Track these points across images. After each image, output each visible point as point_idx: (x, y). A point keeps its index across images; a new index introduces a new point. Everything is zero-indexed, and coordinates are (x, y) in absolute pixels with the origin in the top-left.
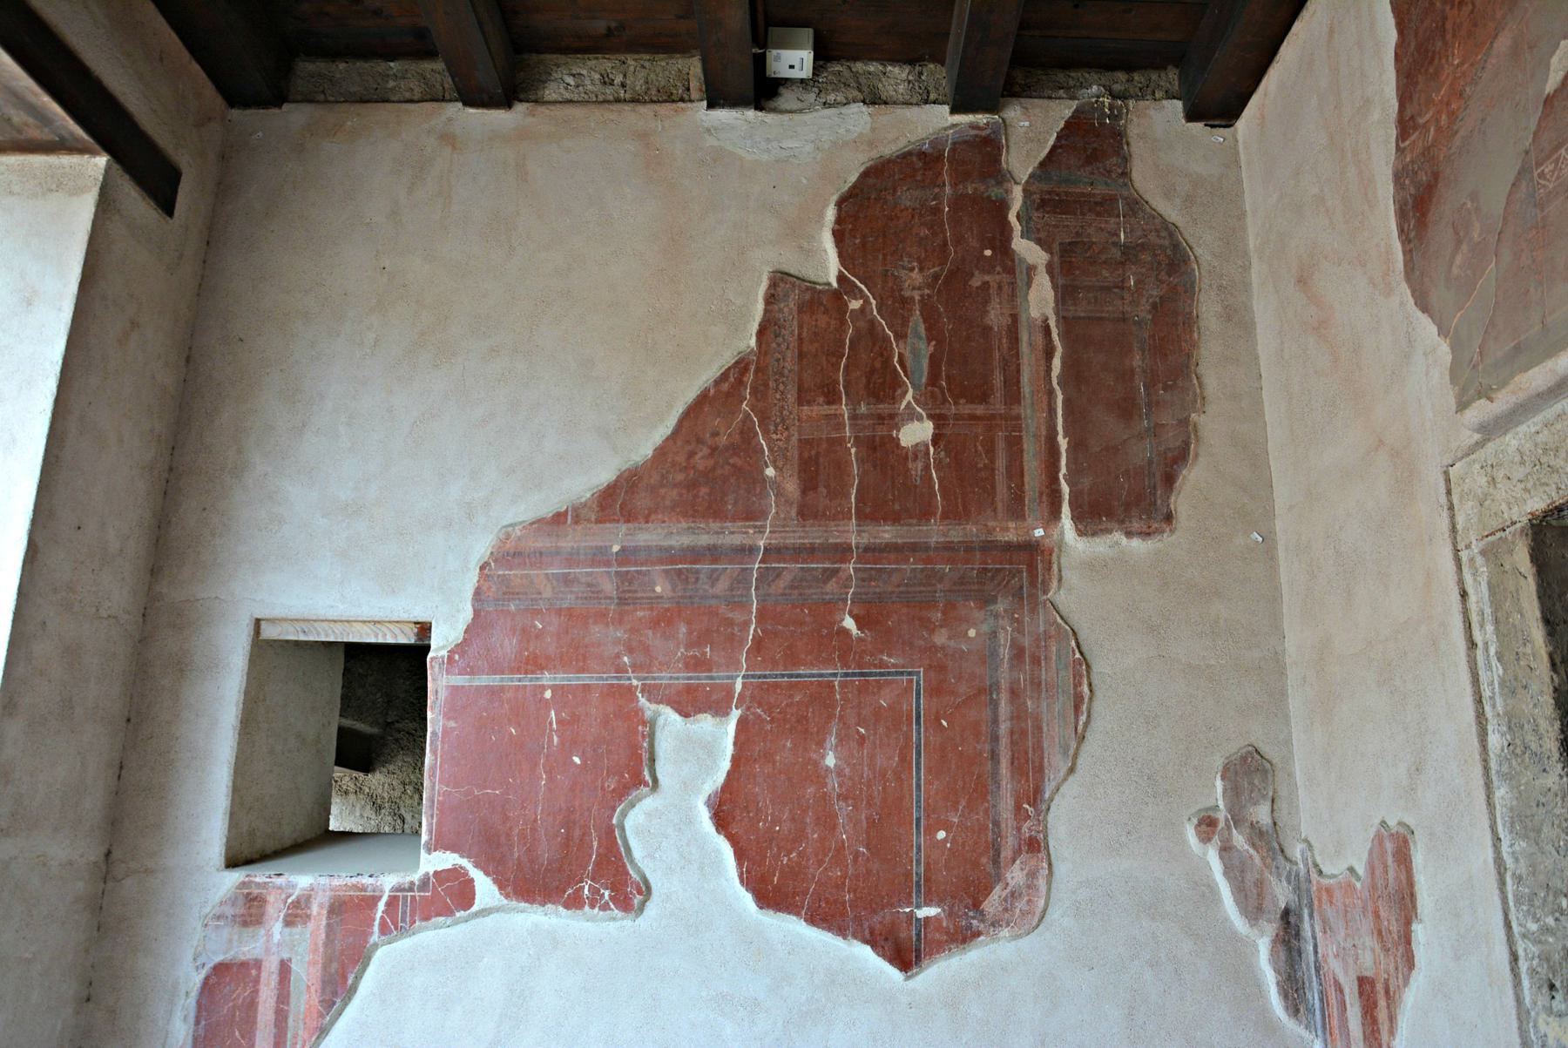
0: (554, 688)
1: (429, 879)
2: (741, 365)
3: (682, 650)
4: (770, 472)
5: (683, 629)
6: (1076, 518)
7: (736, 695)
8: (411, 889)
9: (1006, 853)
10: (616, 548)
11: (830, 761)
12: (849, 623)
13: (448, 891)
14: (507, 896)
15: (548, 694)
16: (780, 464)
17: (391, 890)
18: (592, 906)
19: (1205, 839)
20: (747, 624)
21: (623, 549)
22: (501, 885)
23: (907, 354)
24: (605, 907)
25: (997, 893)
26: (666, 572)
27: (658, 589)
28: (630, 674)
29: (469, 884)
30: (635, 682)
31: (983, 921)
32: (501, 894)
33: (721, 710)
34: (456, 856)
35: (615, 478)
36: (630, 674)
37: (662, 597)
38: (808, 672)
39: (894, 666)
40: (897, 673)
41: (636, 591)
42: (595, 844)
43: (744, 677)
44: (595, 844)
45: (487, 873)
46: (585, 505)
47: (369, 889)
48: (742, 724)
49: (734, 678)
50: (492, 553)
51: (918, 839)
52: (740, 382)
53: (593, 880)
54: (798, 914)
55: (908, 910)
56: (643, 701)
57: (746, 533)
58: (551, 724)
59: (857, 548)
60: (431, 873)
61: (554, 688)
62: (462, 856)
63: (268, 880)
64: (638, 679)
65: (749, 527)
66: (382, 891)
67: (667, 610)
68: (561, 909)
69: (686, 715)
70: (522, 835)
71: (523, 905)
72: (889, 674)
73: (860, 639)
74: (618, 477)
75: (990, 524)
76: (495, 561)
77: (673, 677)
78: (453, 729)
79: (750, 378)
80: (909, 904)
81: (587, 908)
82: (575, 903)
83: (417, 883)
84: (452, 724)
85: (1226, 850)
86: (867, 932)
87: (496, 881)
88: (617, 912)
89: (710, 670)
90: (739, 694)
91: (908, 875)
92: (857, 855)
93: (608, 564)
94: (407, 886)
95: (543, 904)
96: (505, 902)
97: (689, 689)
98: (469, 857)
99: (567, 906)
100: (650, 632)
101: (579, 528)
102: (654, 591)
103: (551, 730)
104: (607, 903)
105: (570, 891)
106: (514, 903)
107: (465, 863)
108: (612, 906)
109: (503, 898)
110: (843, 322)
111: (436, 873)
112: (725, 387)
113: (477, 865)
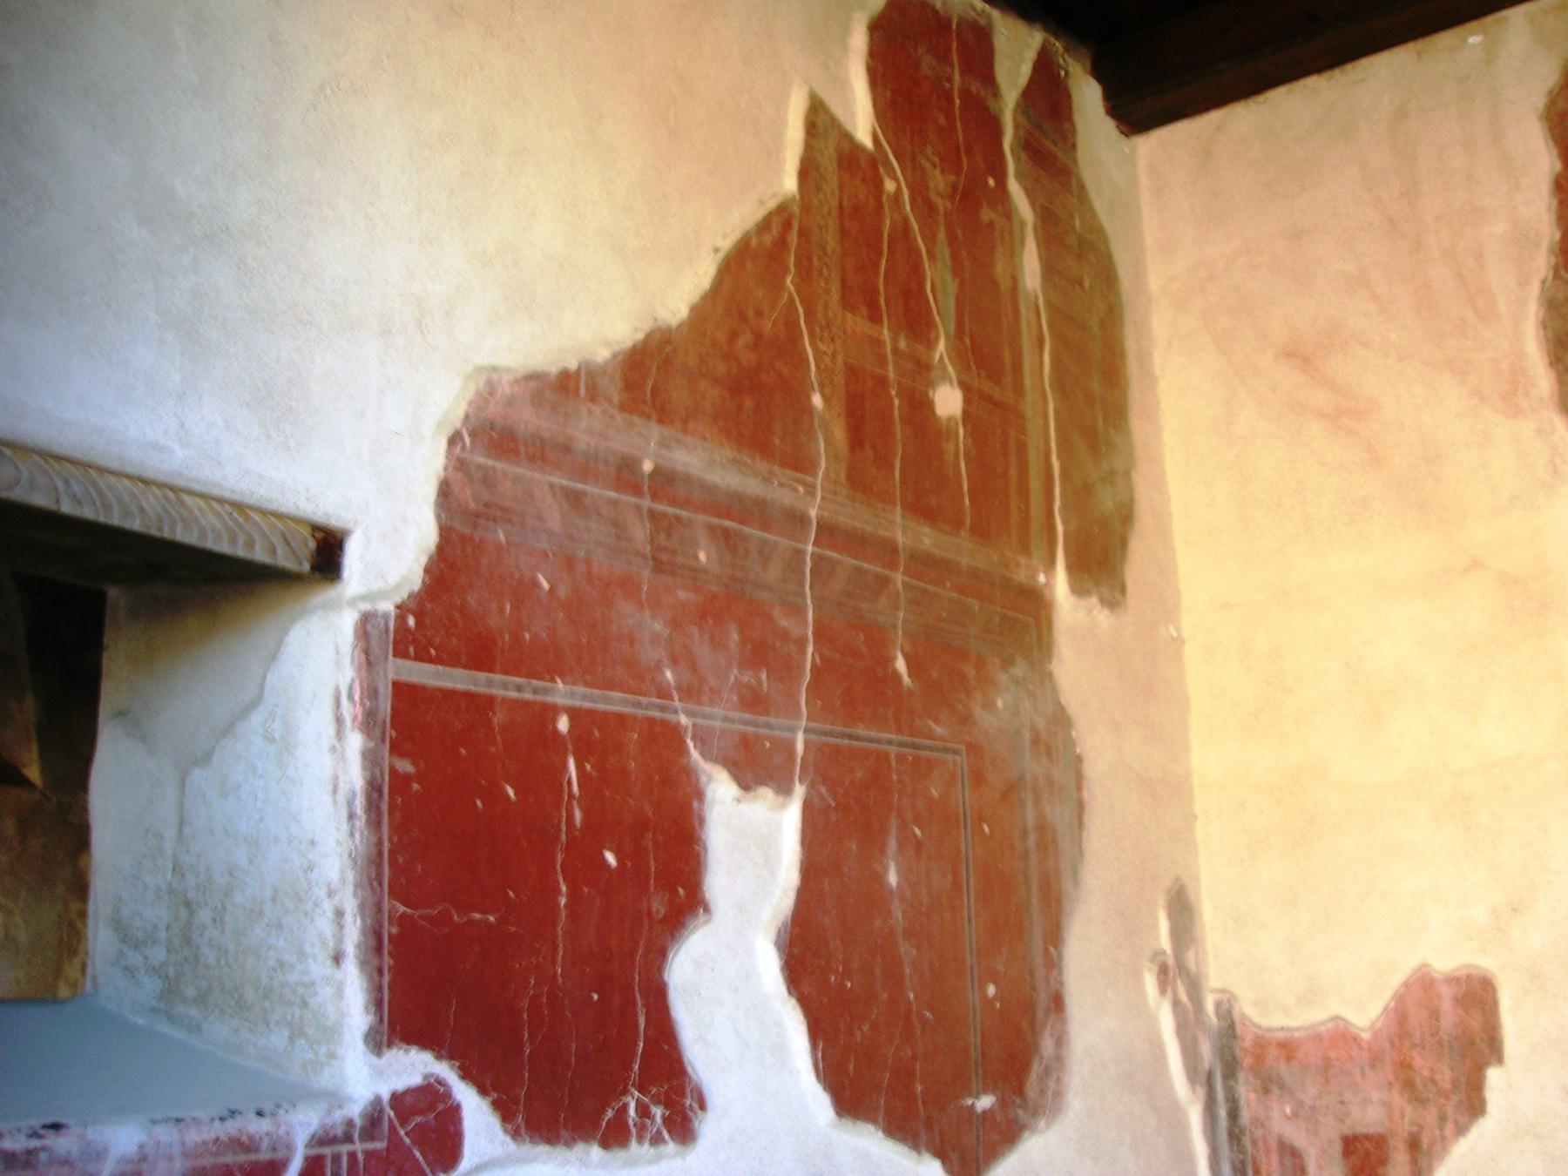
0: (574, 714)
1: (381, 1111)
2: (780, 219)
3: (735, 671)
4: (817, 400)
5: (735, 636)
6: (1070, 569)
7: (799, 760)
8: (348, 1138)
9: (1040, 1015)
10: (648, 466)
11: (893, 878)
12: (901, 665)
13: (420, 1136)
14: (516, 1135)
15: (563, 724)
16: (828, 390)
17: (309, 1145)
18: (640, 1139)
19: (1162, 990)
20: (801, 643)
21: (657, 471)
22: (505, 1110)
23: (938, 285)
24: (657, 1140)
25: (1036, 1069)
26: (712, 529)
27: (702, 556)
28: (677, 703)
29: (453, 1113)
30: (684, 720)
31: (1026, 1109)
32: (506, 1131)
33: (785, 790)
34: (427, 1057)
35: (640, 336)
36: (677, 703)
37: (706, 571)
38: (873, 734)
39: (942, 739)
40: (946, 750)
41: (674, 552)
42: (642, 1021)
43: (806, 731)
44: (642, 1021)
45: (483, 1091)
46: (604, 369)
47: (265, 1145)
48: (807, 807)
49: (793, 730)
50: (467, 417)
51: (973, 998)
52: (782, 243)
53: (642, 1090)
54: (874, 1121)
55: (970, 1102)
56: (695, 754)
57: (796, 490)
58: (570, 783)
59: (904, 550)
60: (386, 1097)
61: (574, 714)
62: (439, 1057)
63: (35, 1143)
64: (689, 714)
65: (798, 481)
66: (290, 1147)
67: (715, 597)
68: (596, 1152)
69: (745, 786)
70: (535, 1008)
71: (543, 1149)
72: (937, 749)
73: (911, 693)
74: (649, 336)
75: (1009, 554)
76: (474, 434)
77: (722, 716)
78: (407, 779)
79: (793, 238)
80: (970, 1094)
81: (634, 1144)
82: (615, 1136)
83: (358, 1122)
84: (405, 766)
85: (1176, 1003)
86: (937, 1140)
87: (498, 1106)
88: (671, 1147)
89: (766, 712)
90: (802, 759)
91: (966, 1050)
92: (923, 1020)
93: (636, 490)
94: (339, 1131)
95: (569, 1144)
96: (511, 1146)
97: (746, 743)
98: (451, 1057)
99: (606, 1144)
100: (695, 631)
101: (597, 410)
102: (697, 558)
103: (571, 795)
104: (659, 1132)
105: (610, 1114)
106: (528, 1149)
107: (445, 1071)
108: (666, 1135)
109: (508, 1139)
110: (880, 206)
111: (396, 1098)
112: (768, 240)
113: (466, 1075)
